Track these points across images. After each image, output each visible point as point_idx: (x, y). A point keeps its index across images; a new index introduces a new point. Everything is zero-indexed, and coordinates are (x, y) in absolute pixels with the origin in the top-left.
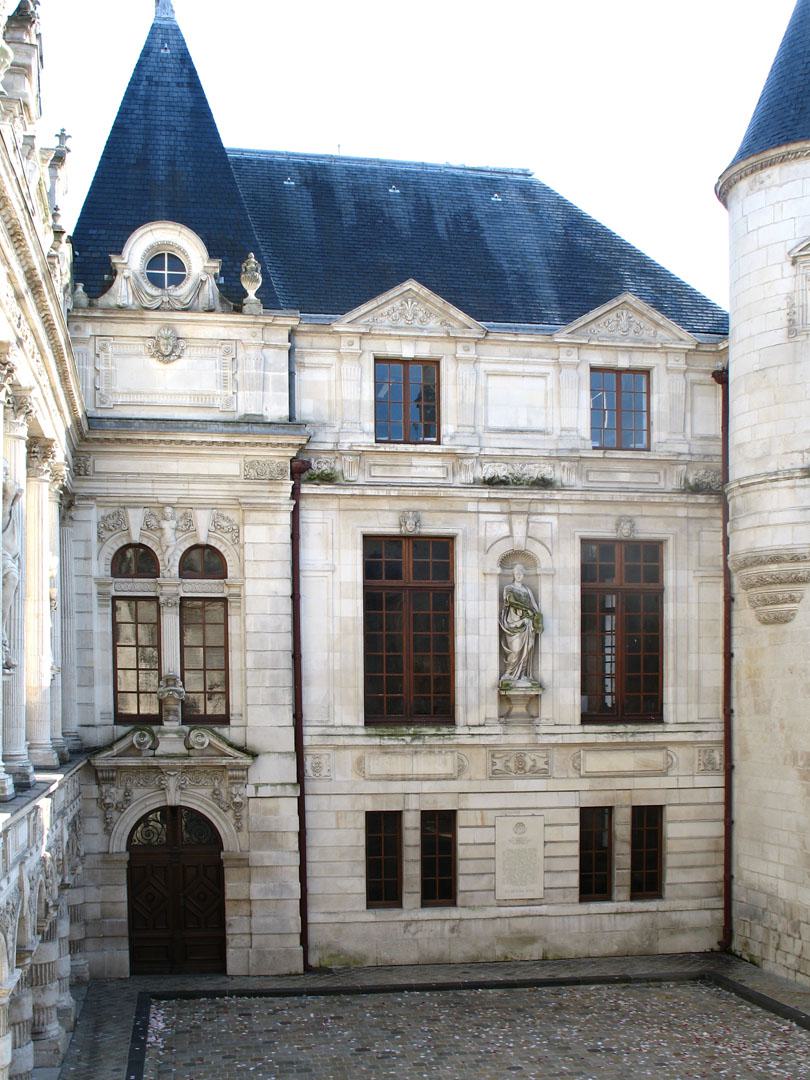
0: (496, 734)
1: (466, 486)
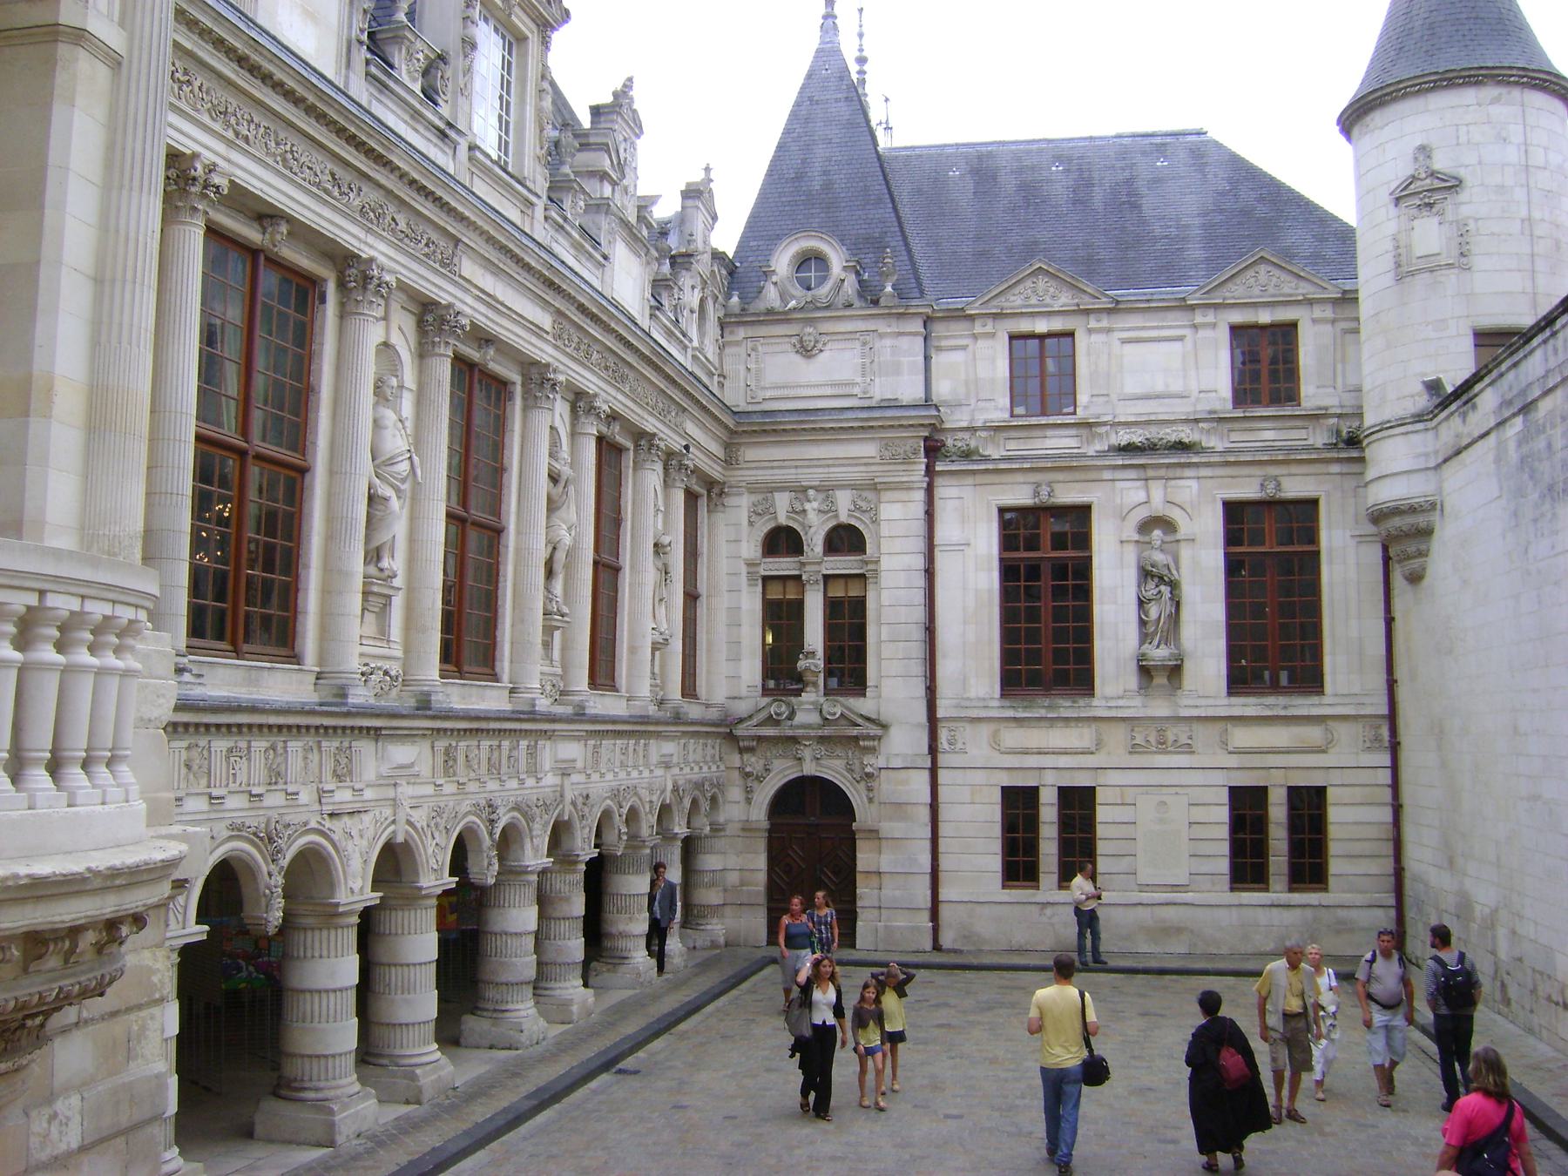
0: (1135, 706)
1: (1101, 455)
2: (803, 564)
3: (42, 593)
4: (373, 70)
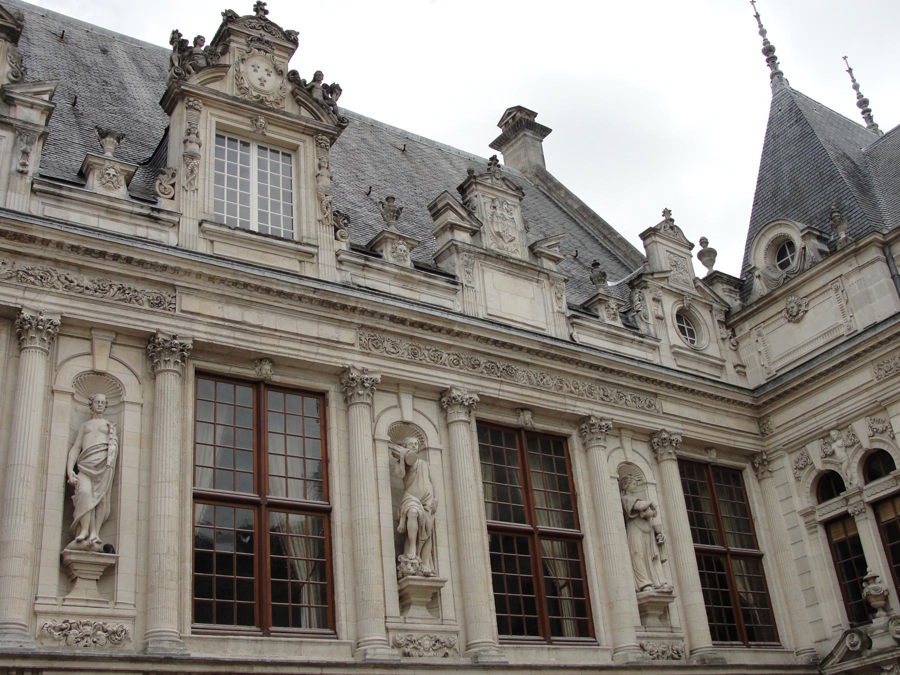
2: (847, 499)
4: (36, 186)
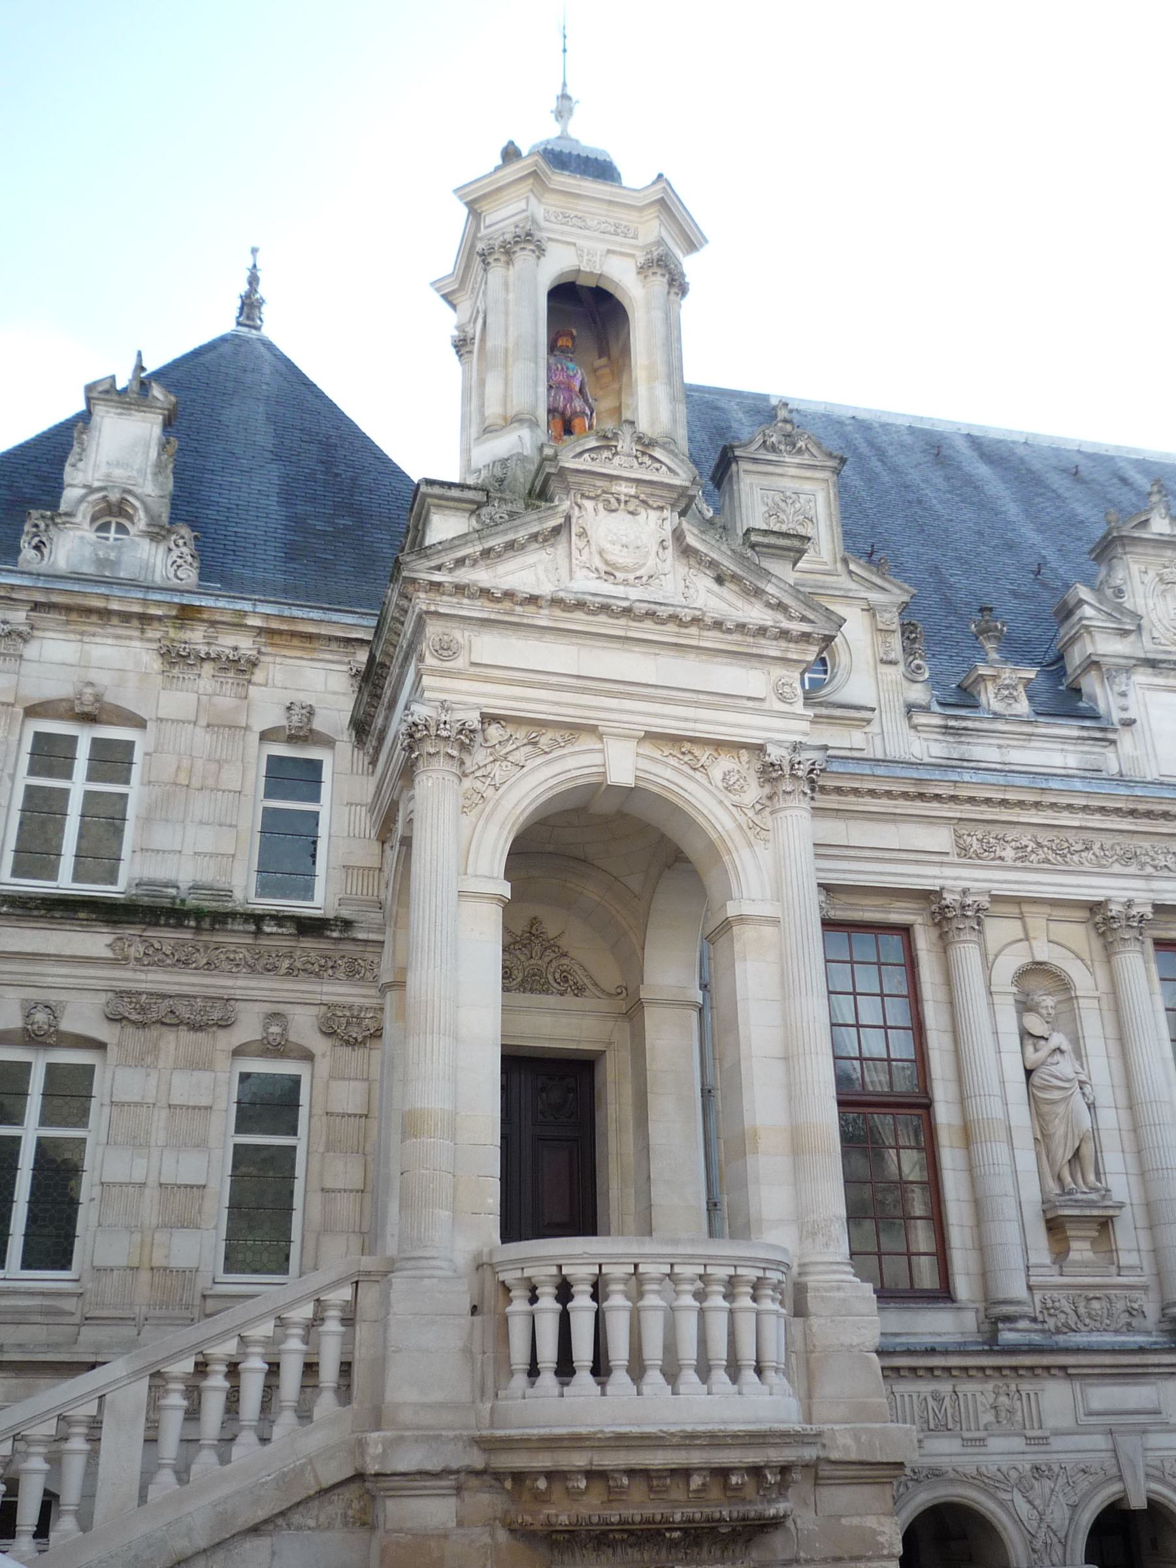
3: (672, 1265)
